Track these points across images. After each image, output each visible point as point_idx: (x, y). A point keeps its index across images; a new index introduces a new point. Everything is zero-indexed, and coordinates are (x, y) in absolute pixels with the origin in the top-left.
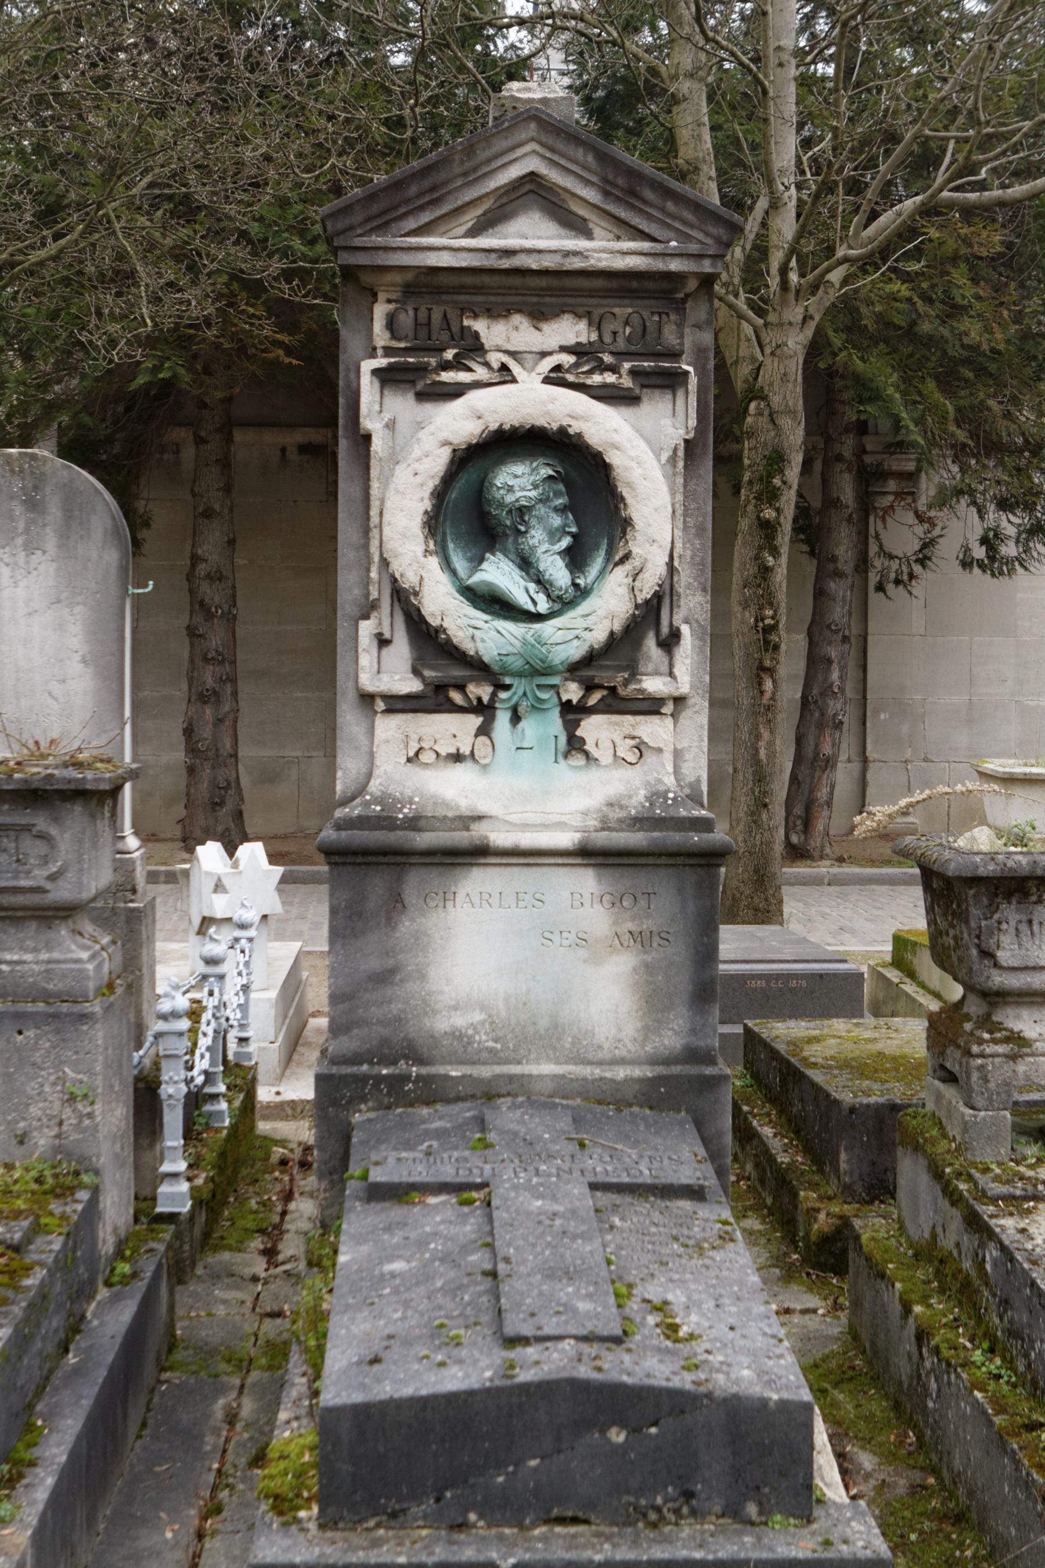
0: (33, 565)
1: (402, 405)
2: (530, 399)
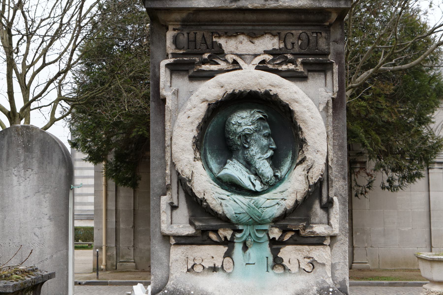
0: (27, 176)
1: (182, 83)
2: (250, 78)
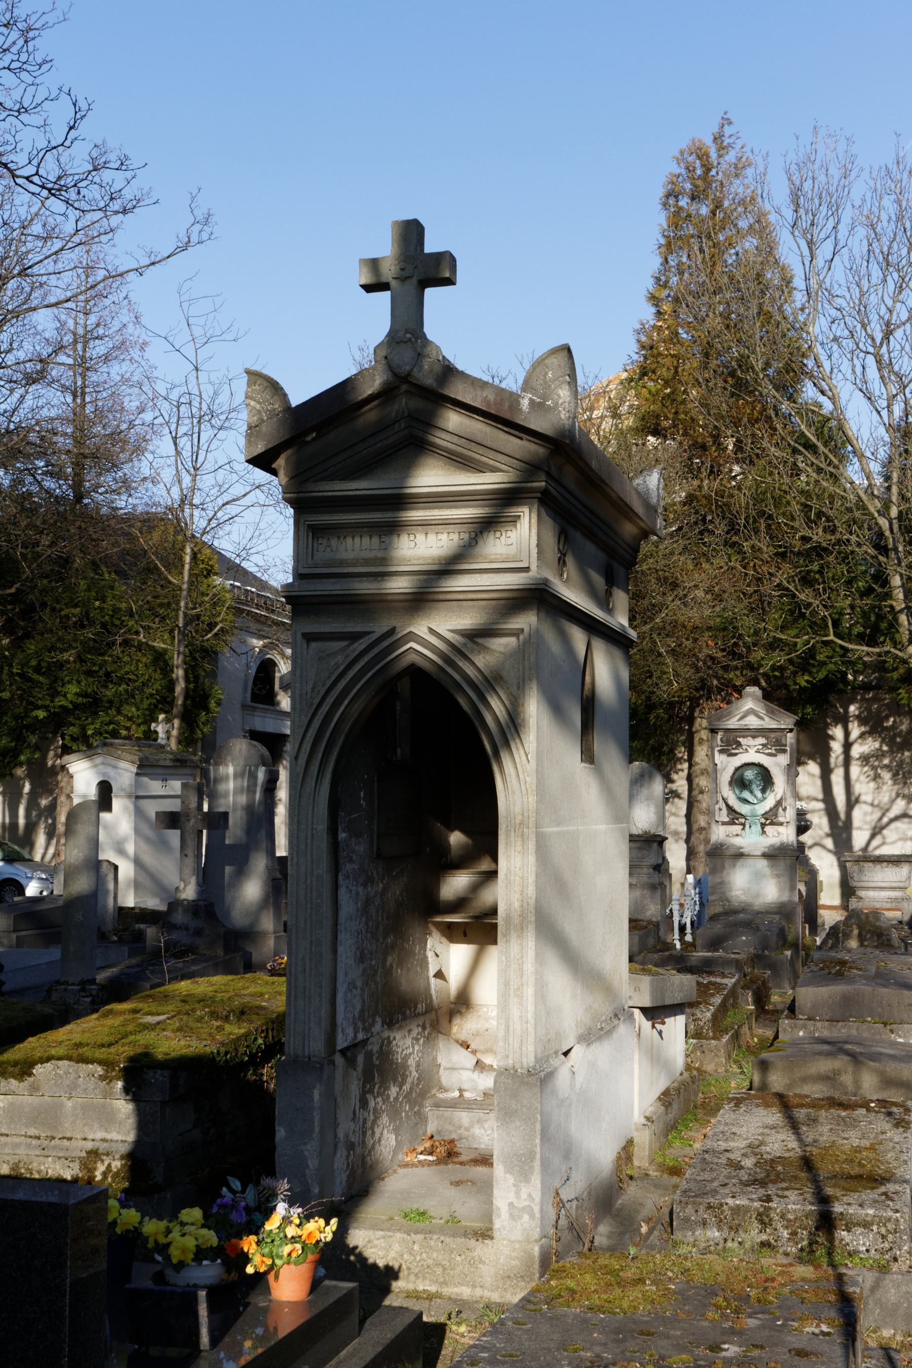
1: (724, 757)
2: (752, 756)
